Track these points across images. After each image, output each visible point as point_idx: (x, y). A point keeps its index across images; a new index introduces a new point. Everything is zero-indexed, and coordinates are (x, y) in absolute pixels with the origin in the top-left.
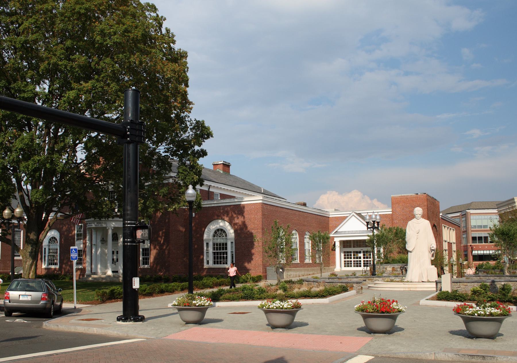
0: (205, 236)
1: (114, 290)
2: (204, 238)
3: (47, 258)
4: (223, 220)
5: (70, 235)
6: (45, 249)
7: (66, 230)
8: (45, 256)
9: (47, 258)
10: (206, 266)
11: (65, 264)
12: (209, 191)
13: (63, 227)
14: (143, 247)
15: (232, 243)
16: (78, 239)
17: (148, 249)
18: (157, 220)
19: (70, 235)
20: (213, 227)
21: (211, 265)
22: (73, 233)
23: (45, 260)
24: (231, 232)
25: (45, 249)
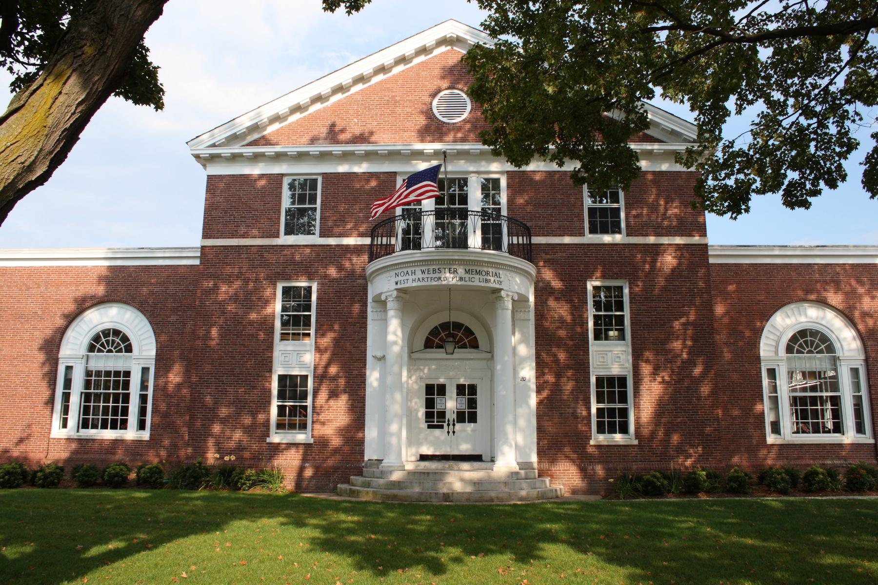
0: (765, 349)
1: (719, 536)
2: (762, 354)
3: (75, 400)
4: (823, 303)
5: (253, 316)
6: (69, 369)
7: (235, 298)
8: (66, 397)
9: (75, 400)
10: (771, 439)
11: (224, 421)
12: (530, 244)
13: (216, 288)
14: (603, 373)
15: (855, 372)
16: (284, 337)
17: (622, 380)
18: (661, 281)
19: (253, 316)
20: (785, 322)
21: (789, 433)
22: (269, 310)
23: (66, 410)
24: (847, 340)
25: (69, 369)
